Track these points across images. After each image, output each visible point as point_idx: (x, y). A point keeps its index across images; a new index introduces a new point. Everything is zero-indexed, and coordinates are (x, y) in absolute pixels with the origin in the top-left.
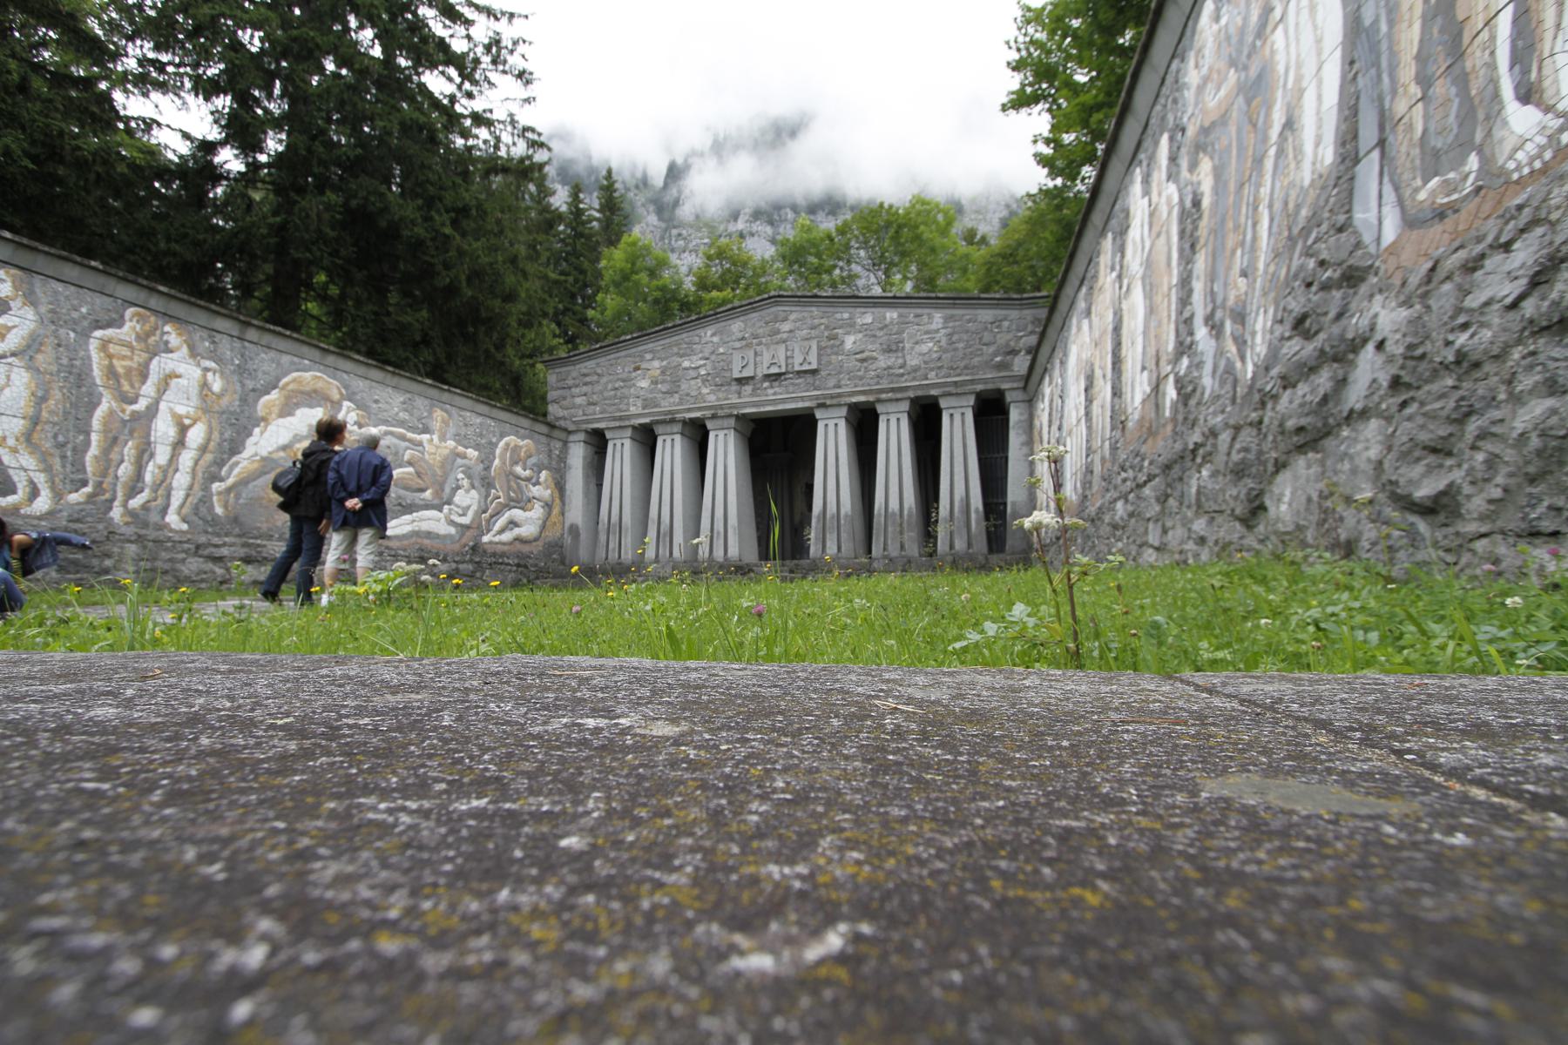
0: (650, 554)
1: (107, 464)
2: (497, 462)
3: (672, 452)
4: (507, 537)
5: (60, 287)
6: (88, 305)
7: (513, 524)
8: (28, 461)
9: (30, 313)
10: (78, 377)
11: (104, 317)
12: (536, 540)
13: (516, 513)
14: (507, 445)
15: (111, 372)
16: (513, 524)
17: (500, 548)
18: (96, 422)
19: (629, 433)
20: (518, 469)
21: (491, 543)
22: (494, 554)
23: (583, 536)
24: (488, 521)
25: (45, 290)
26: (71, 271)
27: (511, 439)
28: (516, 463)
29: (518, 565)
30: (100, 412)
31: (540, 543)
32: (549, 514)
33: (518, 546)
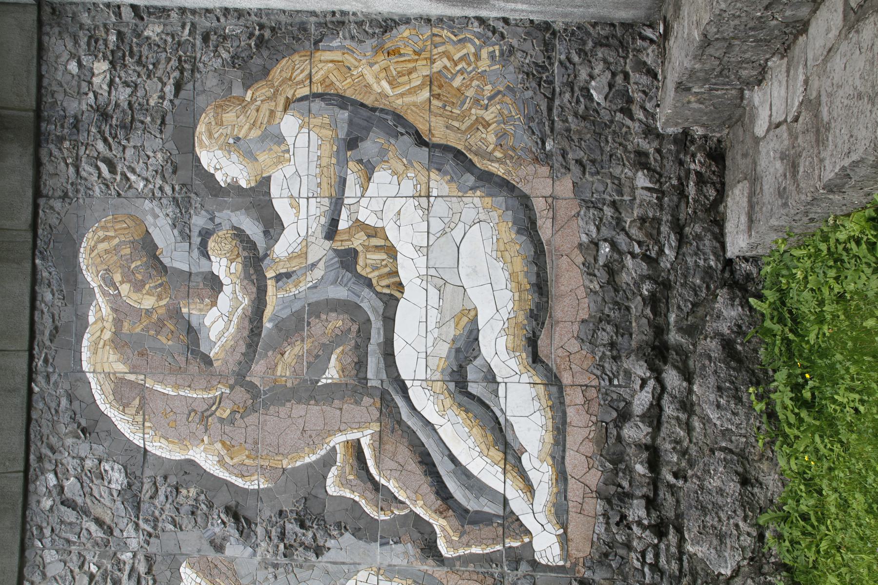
2: (206, 459)
4: (524, 407)
7: (463, 374)
12: (528, 226)
13: (417, 345)
14: (122, 392)
16: (463, 374)
17: (585, 471)
20: (219, 323)
21: (560, 513)
22: (614, 498)
24: (467, 519)
27: (98, 360)
28: (192, 334)
29: (658, 353)
31: (538, 184)
32: (398, 124)
33: (563, 341)
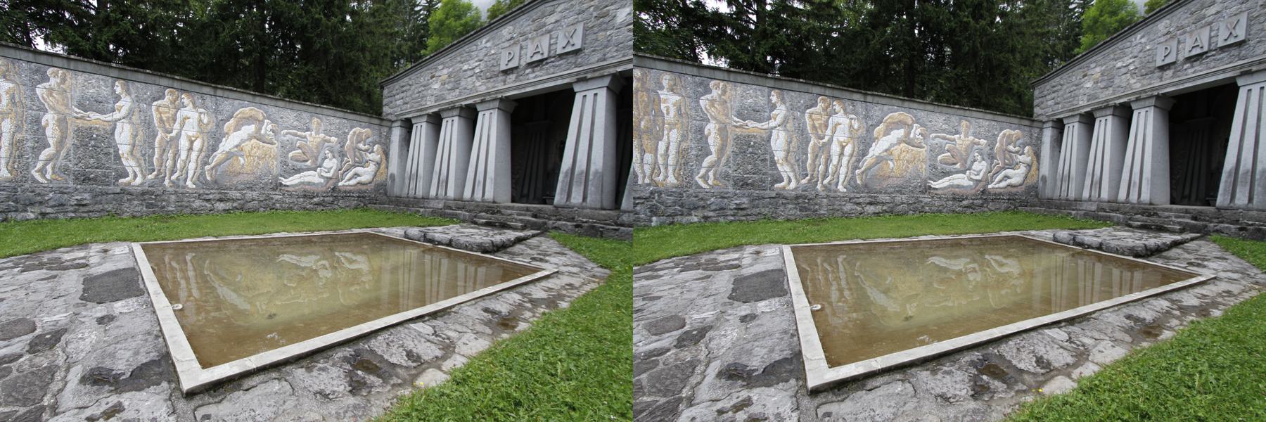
0: (433, 193)
1: (162, 162)
3: (452, 128)
5: (138, 85)
6: (150, 91)
8: (132, 163)
9: (128, 99)
10: (148, 124)
11: (157, 95)
15: (161, 120)
18: (157, 144)
19: (425, 119)
23: (397, 180)
25: (133, 87)
26: (141, 77)
30: (158, 138)
